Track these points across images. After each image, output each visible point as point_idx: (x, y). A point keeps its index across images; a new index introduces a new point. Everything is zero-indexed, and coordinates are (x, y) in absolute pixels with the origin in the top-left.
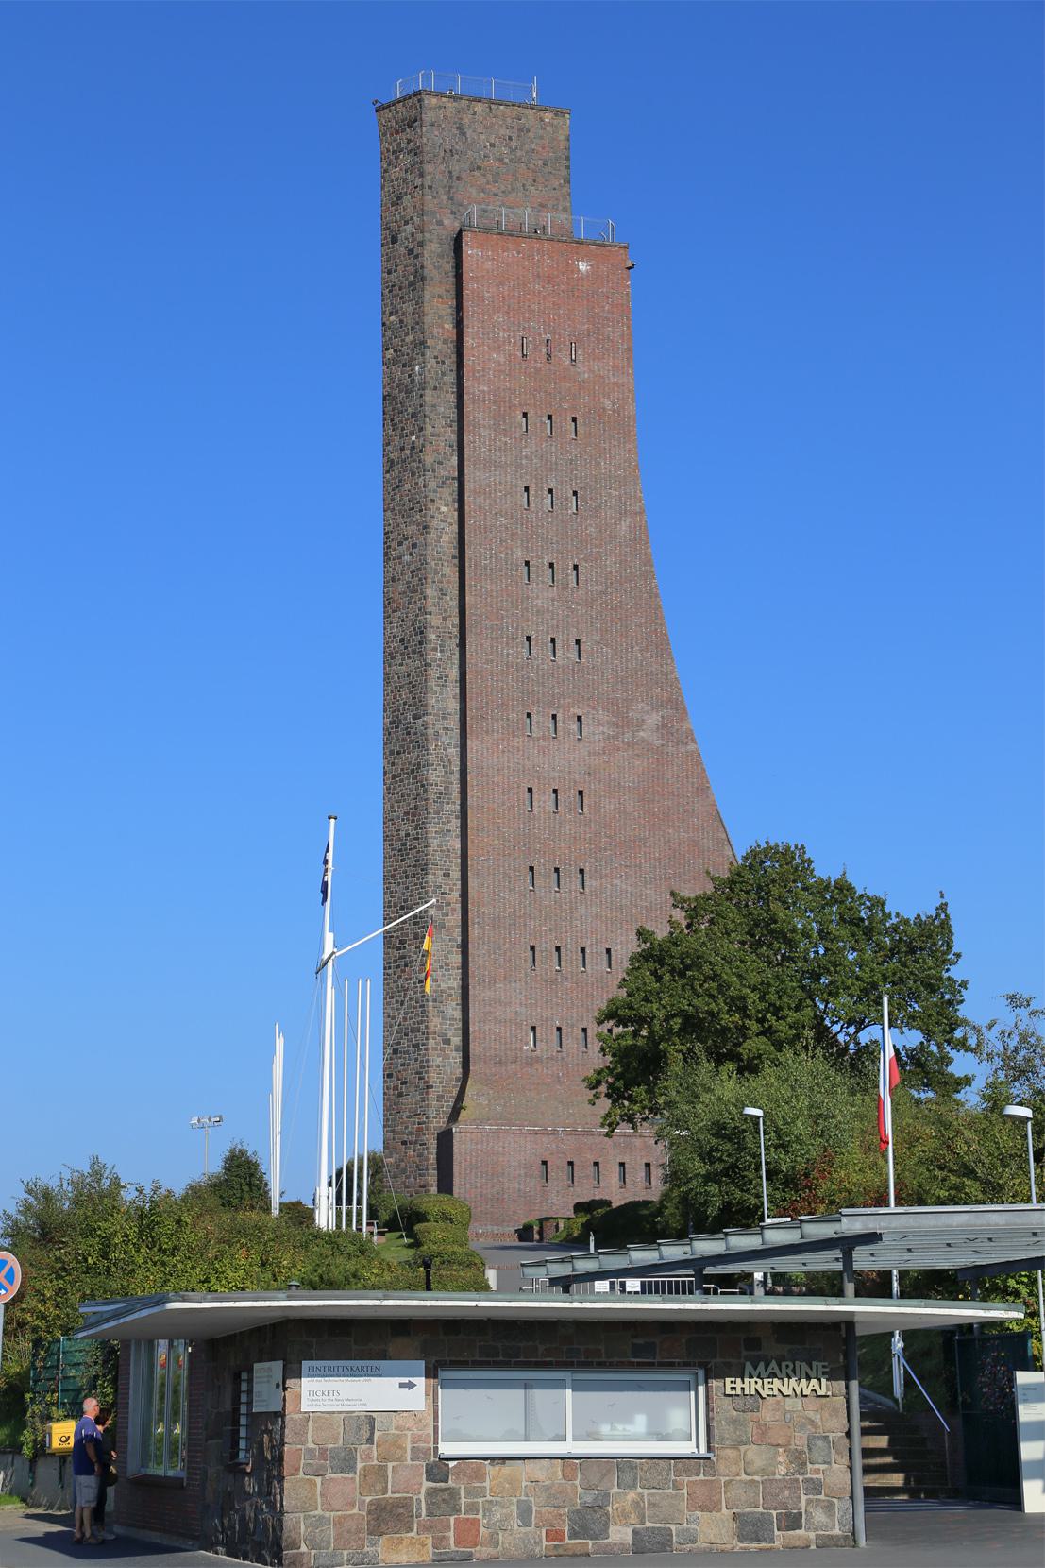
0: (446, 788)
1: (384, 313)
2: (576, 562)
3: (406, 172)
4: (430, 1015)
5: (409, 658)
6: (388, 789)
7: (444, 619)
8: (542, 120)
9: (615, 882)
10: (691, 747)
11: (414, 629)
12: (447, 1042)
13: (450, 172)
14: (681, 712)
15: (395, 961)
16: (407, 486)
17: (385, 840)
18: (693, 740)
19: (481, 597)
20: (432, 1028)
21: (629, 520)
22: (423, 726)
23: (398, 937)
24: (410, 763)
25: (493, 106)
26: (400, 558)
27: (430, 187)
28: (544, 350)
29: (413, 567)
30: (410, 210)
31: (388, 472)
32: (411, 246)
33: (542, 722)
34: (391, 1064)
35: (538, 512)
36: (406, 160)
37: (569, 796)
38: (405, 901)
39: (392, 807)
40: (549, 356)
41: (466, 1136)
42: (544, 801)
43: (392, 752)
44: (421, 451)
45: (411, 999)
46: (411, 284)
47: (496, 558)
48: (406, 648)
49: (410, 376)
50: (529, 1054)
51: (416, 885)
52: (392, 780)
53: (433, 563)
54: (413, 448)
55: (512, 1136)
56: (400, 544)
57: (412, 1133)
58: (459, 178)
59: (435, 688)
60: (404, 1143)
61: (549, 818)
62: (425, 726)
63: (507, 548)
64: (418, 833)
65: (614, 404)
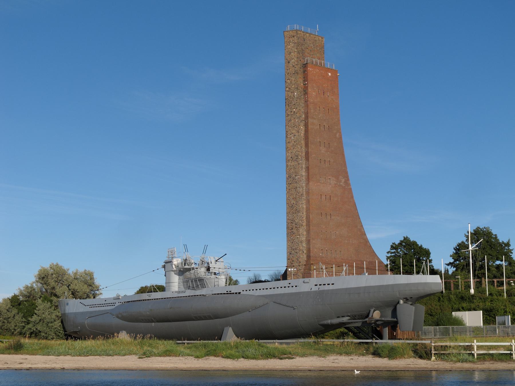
0: (303, 193)
3: (292, 47)
5: (294, 162)
6: (288, 192)
7: (302, 153)
8: (319, 39)
9: (337, 217)
10: (350, 187)
11: (295, 155)
12: (303, 252)
13: (302, 49)
14: (348, 180)
16: (293, 121)
18: (350, 186)
23: (291, 227)
24: (294, 187)
26: (291, 138)
29: (294, 140)
30: (293, 56)
32: (294, 65)
37: (328, 197)
38: (293, 219)
39: (289, 196)
42: (323, 197)
43: (289, 183)
45: (295, 242)
46: (293, 74)
49: (293, 95)
51: (296, 215)
54: (294, 112)
56: (291, 134)
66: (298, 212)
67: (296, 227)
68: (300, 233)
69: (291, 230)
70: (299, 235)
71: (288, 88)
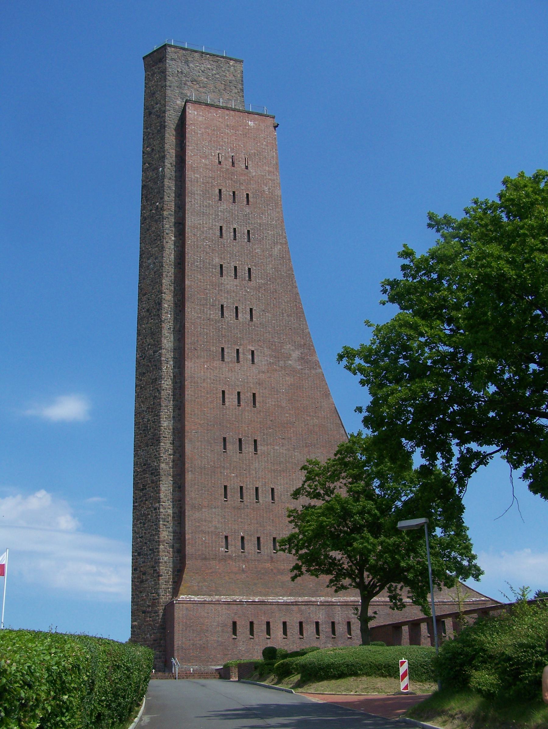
1: (143, 148)
2: (249, 266)
4: (161, 530)
5: (152, 319)
6: (138, 395)
9: (276, 448)
10: (319, 371)
11: (155, 303)
15: (140, 498)
16: (153, 229)
17: (135, 425)
18: (320, 367)
19: (194, 282)
20: (162, 539)
21: (279, 247)
22: (159, 356)
25: (203, 55)
27: (170, 87)
28: (231, 160)
31: (143, 224)
33: (230, 355)
34: (136, 562)
35: (227, 239)
36: (157, 77)
37: (246, 397)
40: (233, 163)
41: (183, 606)
42: (232, 399)
44: (161, 209)
47: (204, 261)
48: (150, 314)
50: (224, 554)
52: (140, 388)
53: (167, 266)
55: (213, 605)
56: (148, 259)
57: (149, 606)
58: (185, 84)
59: (167, 334)
60: (144, 612)
61: (235, 409)
62: (160, 355)
63: (209, 257)
64: (154, 419)
65: (269, 189)
67: (153, 482)
69: (143, 490)
71: (147, 164)
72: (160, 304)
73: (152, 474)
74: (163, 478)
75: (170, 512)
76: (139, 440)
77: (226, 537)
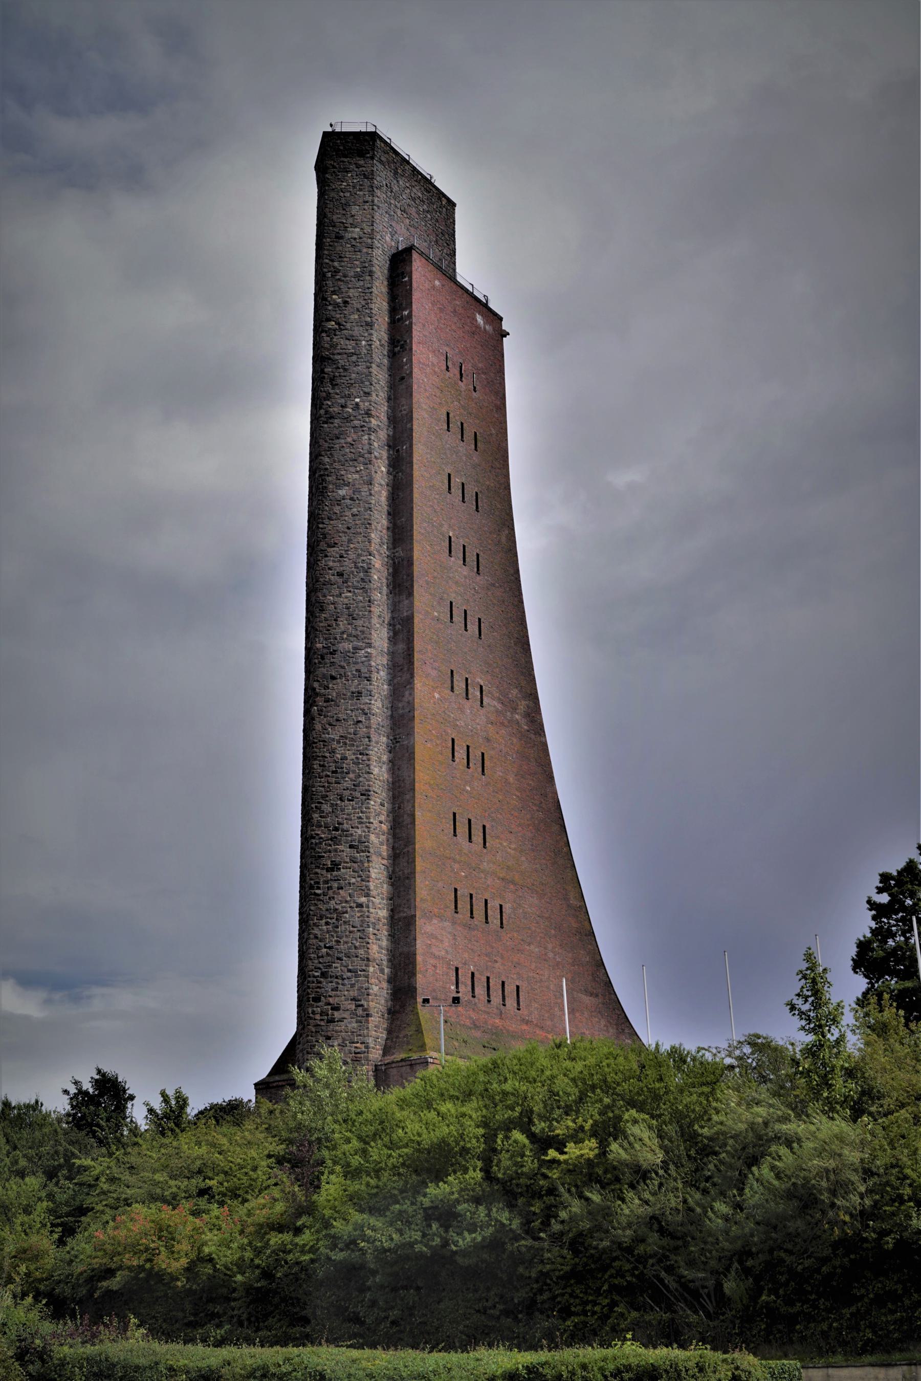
62: (368, 656)
64: (357, 758)
66: (362, 795)
68: (372, 885)
70: (367, 895)
72: (367, 571)
73: (351, 847)
74: (374, 858)
75: (383, 913)
76: (323, 786)
77: (457, 969)
